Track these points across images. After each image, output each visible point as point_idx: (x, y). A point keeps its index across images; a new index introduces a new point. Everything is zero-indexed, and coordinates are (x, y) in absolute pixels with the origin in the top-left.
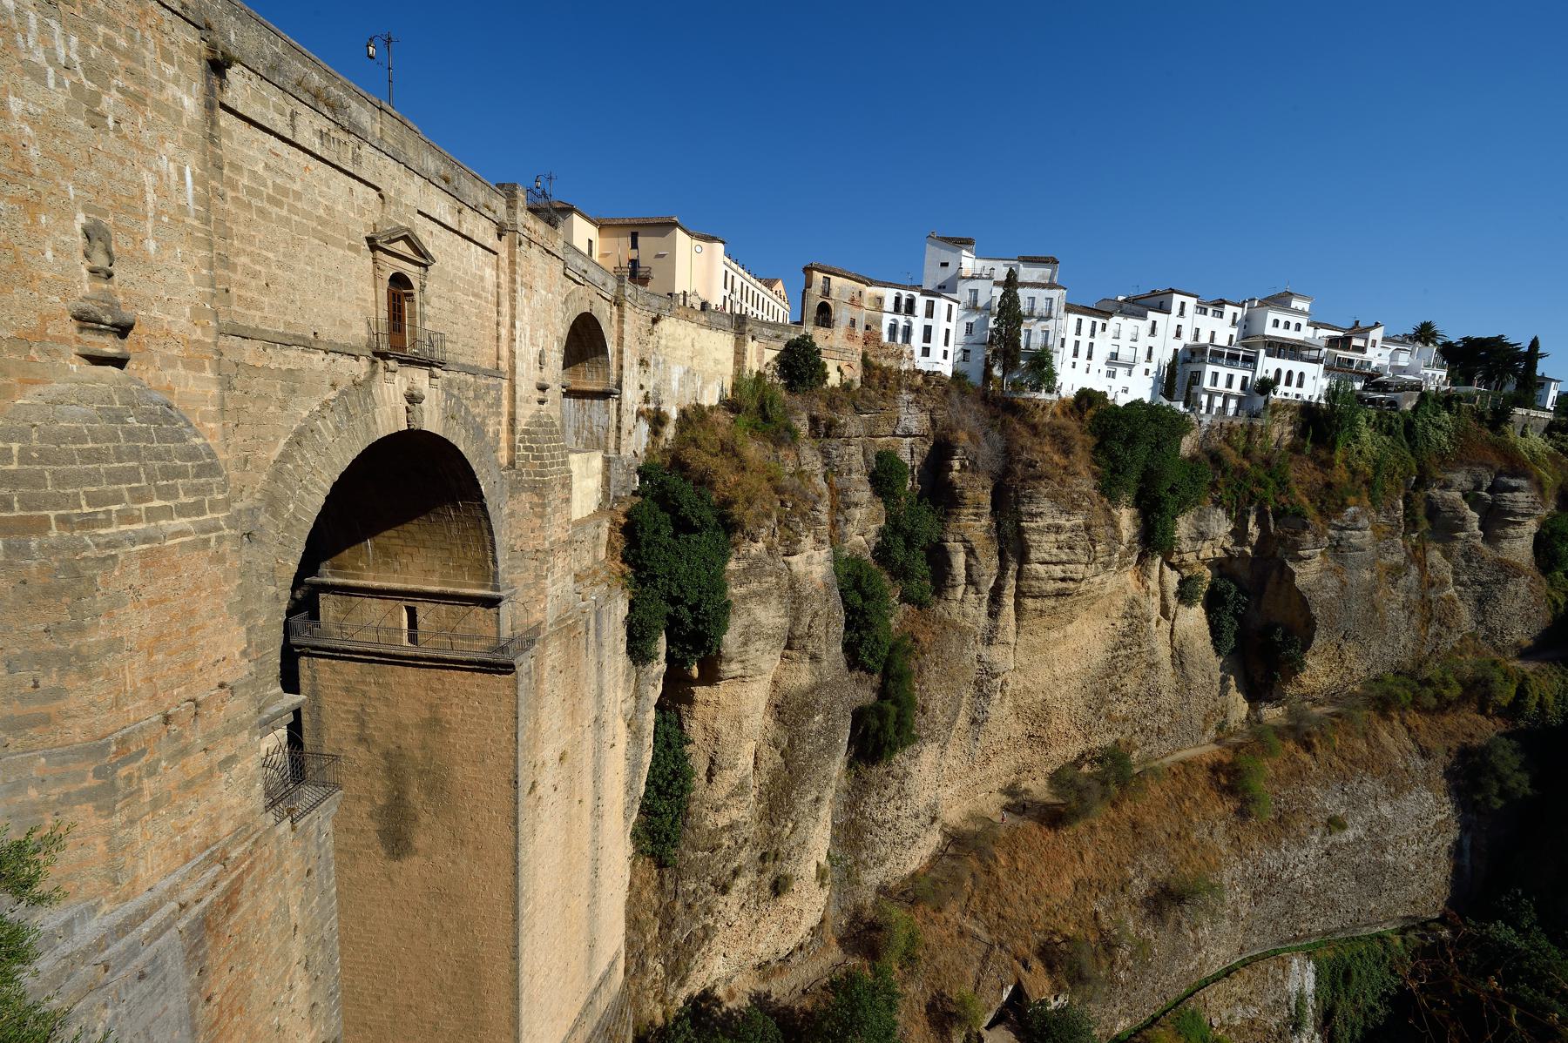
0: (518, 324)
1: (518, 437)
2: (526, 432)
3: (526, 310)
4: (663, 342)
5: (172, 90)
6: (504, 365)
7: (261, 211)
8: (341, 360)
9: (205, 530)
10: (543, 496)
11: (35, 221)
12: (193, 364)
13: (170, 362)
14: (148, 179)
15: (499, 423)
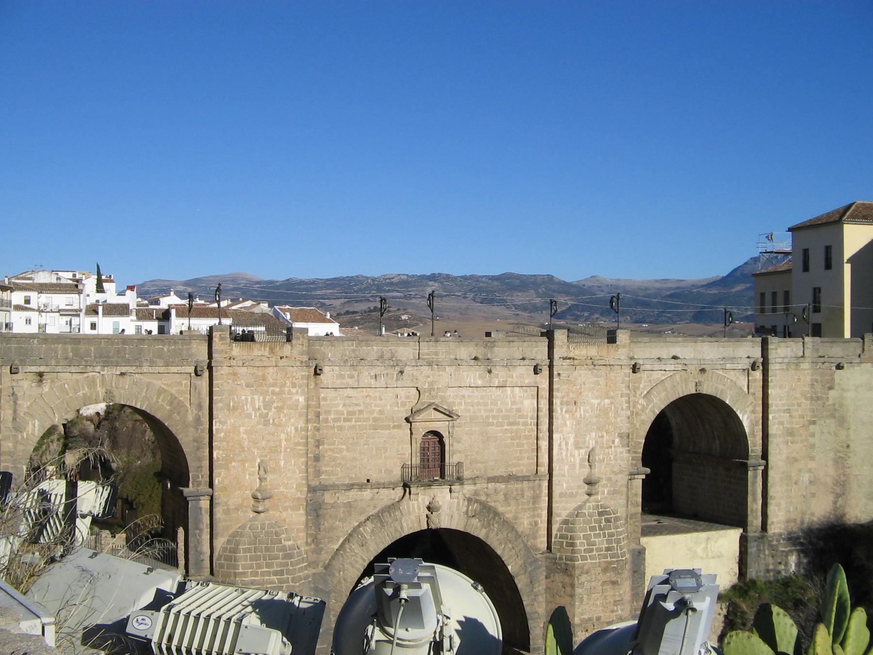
0: (555, 436)
1: (555, 528)
2: (565, 522)
3: (568, 423)
4: (849, 395)
5: (295, 397)
6: (544, 469)
7: (341, 428)
8: (382, 491)
9: (280, 582)
10: (571, 576)
11: (244, 466)
12: (295, 508)
13: (286, 509)
14: (283, 436)
15: (539, 516)
